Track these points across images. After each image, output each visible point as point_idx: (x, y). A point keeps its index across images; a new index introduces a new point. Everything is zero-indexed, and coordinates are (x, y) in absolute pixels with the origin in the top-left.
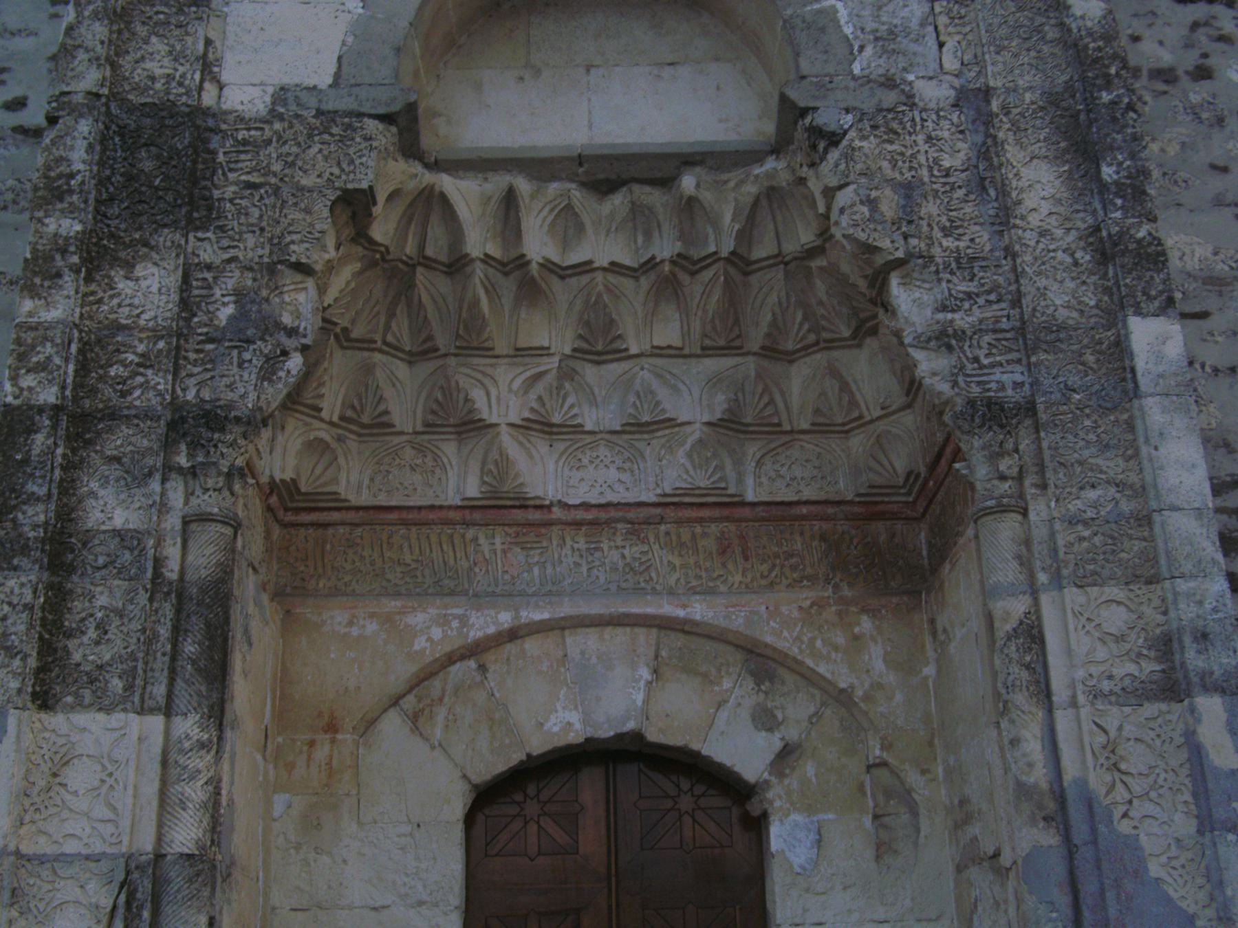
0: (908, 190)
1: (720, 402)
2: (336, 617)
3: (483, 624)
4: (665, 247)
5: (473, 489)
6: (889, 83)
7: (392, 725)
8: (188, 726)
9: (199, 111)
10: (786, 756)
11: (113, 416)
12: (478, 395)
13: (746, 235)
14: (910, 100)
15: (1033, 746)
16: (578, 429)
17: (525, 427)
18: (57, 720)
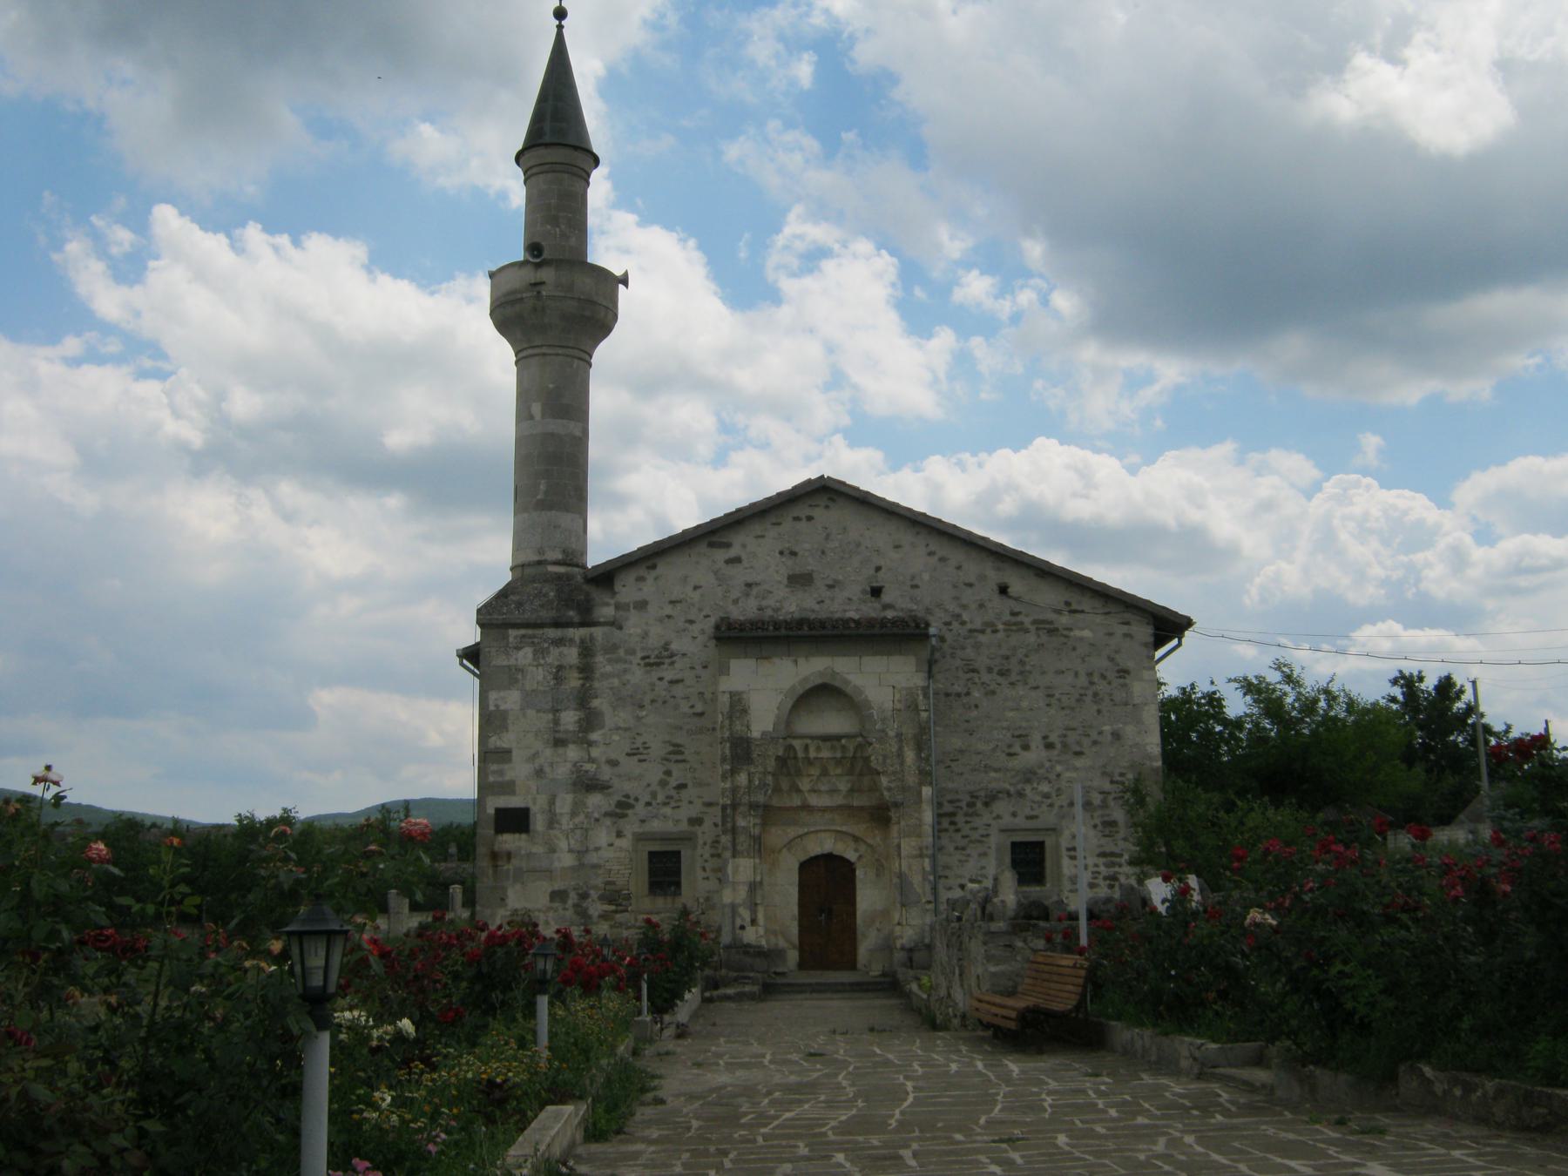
0: (885, 757)
1: (849, 785)
2: (773, 830)
3: (801, 831)
4: (839, 755)
5: (799, 803)
6: (883, 731)
7: (785, 850)
8: (757, 861)
9: (748, 738)
11: (739, 804)
12: (800, 785)
13: (855, 753)
14: (887, 734)
15: (897, 865)
16: (820, 791)
17: (809, 791)
18: (736, 860)
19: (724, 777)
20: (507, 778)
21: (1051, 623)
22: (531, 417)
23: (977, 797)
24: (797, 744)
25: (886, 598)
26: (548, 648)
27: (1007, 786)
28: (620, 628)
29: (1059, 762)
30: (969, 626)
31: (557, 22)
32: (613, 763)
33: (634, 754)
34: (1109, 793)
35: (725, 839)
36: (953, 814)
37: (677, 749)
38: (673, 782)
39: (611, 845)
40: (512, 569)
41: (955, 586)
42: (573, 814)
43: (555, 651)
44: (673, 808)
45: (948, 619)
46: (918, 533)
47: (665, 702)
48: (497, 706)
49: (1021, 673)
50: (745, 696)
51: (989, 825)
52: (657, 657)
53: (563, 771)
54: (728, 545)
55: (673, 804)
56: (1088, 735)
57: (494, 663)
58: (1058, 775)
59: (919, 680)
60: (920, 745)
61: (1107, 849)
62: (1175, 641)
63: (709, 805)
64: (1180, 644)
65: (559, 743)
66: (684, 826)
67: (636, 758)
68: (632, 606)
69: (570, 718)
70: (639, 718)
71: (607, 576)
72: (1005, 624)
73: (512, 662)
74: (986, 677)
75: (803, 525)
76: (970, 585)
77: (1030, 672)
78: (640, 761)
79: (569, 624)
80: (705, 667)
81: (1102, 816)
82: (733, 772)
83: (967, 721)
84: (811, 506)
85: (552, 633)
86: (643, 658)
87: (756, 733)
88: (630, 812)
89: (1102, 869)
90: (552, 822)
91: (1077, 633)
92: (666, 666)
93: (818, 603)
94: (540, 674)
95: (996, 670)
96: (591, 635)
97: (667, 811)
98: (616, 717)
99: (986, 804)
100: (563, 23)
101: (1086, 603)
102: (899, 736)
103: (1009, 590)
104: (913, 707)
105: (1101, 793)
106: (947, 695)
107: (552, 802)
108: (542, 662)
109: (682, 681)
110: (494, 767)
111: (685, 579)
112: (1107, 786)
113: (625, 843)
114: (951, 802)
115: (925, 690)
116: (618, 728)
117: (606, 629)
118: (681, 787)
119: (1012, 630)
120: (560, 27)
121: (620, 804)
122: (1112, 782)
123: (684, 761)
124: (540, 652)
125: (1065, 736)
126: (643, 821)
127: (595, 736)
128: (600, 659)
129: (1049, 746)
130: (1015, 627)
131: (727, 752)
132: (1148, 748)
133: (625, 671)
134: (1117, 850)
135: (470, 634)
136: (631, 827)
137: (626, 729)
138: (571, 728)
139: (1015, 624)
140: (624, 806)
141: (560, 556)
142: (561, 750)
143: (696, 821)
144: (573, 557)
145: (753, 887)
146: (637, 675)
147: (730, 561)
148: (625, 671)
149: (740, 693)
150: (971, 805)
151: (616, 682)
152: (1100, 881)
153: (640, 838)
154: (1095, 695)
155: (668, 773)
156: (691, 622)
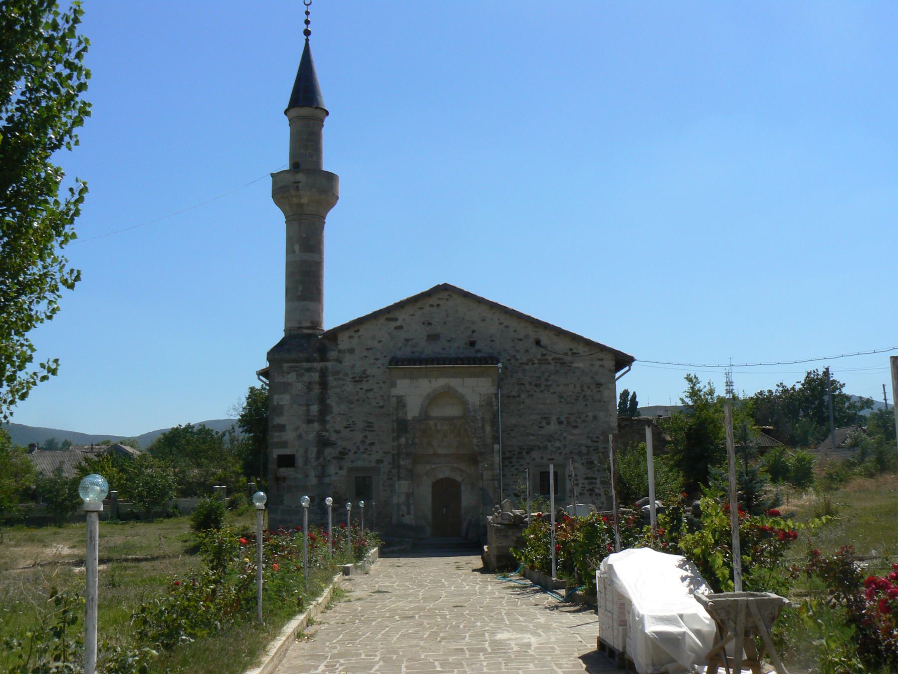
3: (434, 466)
8: (410, 482)
10: (463, 480)
14: (476, 418)
19: (393, 440)
20: (283, 439)
21: (562, 359)
22: (294, 252)
23: (523, 449)
24: (431, 423)
25: (477, 347)
26: (304, 373)
27: (538, 443)
28: (341, 362)
29: (565, 431)
30: (520, 361)
31: (306, 37)
32: (338, 432)
33: (347, 427)
34: (590, 447)
35: (394, 471)
36: (511, 458)
37: (370, 425)
38: (368, 441)
39: (336, 473)
40: (284, 331)
41: (513, 340)
42: (318, 458)
43: (307, 375)
44: (369, 454)
45: (509, 358)
46: (494, 313)
47: (364, 401)
48: (278, 403)
49: (547, 386)
50: (404, 398)
51: (529, 463)
52: (360, 377)
53: (312, 436)
54: (396, 319)
55: (368, 453)
56: (580, 417)
57: (276, 381)
58: (565, 438)
59: (493, 390)
60: (494, 423)
61: (589, 476)
62: (627, 368)
63: (386, 453)
64: (629, 370)
65: (309, 422)
66: (373, 464)
67: (349, 429)
68: (346, 351)
69: (315, 409)
70: (350, 409)
71: (334, 334)
72: (538, 360)
73: (285, 380)
74: (528, 387)
75: (435, 309)
76: (521, 340)
77: (551, 385)
78: (351, 431)
79: (314, 360)
80: (384, 383)
81: (587, 458)
82: (398, 437)
83: (519, 410)
84: (439, 299)
85: (305, 365)
86: (353, 378)
87: (410, 417)
88: (346, 457)
89: (586, 485)
90: (306, 462)
91: (575, 365)
92: (364, 382)
93: (443, 349)
94: (300, 386)
95: (533, 384)
96: (326, 367)
97: (365, 456)
98: (336, 408)
99: (528, 453)
100: (309, 38)
101: (581, 349)
102: (483, 418)
103: (541, 343)
104: (490, 404)
105: (586, 447)
106: (509, 397)
107: (306, 452)
108: (301, 380)
109: (373, 390)
110: (277, 434)
111: (374, 337)
112: (590, 443)
113: (343, 472)
114: (509, 452)
115: (496, 395)
116: (340, 414)
117: (333, 363)
118: (372, 444)
119: (542, 364)
120: (307, 40)
121: (341, 453)
122: (592, 441)
123: (373, 431)
124: (300, 375)
125: (568, 418)
126: (353, 461)
127: (328, 418)
128: (330, 378)
129: (560, 423)
130: (543, 361)
131: (395, 427)
132: (611, 423)
133: (343, 385)
134: (594, 476)
135: (265, 364)
136: (347, 464)
137: (344, 414)
138: (316, 414)
139: (544, 360)
140: (343, 454)
141: (309, 325)
142: (311, 425)
143: (379, 462)
144: (316, 324)
145: (408, 496)
146: (349, 387)
147: (397, 328)
148: (343, 385)
149: (401, 397)
150: (520, 453)
151: (339, 390)
152: (585, 492)
153: (351, 470)
154: (585, 396)
155: (366, 437)
156: (377, 359)
